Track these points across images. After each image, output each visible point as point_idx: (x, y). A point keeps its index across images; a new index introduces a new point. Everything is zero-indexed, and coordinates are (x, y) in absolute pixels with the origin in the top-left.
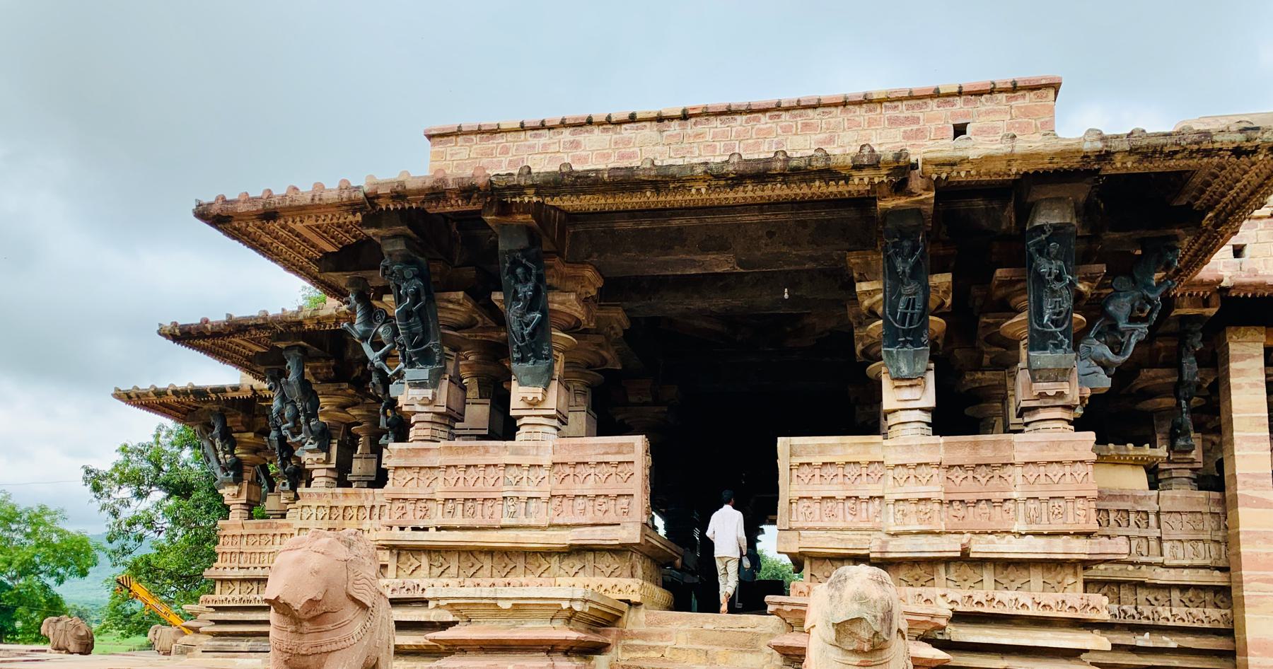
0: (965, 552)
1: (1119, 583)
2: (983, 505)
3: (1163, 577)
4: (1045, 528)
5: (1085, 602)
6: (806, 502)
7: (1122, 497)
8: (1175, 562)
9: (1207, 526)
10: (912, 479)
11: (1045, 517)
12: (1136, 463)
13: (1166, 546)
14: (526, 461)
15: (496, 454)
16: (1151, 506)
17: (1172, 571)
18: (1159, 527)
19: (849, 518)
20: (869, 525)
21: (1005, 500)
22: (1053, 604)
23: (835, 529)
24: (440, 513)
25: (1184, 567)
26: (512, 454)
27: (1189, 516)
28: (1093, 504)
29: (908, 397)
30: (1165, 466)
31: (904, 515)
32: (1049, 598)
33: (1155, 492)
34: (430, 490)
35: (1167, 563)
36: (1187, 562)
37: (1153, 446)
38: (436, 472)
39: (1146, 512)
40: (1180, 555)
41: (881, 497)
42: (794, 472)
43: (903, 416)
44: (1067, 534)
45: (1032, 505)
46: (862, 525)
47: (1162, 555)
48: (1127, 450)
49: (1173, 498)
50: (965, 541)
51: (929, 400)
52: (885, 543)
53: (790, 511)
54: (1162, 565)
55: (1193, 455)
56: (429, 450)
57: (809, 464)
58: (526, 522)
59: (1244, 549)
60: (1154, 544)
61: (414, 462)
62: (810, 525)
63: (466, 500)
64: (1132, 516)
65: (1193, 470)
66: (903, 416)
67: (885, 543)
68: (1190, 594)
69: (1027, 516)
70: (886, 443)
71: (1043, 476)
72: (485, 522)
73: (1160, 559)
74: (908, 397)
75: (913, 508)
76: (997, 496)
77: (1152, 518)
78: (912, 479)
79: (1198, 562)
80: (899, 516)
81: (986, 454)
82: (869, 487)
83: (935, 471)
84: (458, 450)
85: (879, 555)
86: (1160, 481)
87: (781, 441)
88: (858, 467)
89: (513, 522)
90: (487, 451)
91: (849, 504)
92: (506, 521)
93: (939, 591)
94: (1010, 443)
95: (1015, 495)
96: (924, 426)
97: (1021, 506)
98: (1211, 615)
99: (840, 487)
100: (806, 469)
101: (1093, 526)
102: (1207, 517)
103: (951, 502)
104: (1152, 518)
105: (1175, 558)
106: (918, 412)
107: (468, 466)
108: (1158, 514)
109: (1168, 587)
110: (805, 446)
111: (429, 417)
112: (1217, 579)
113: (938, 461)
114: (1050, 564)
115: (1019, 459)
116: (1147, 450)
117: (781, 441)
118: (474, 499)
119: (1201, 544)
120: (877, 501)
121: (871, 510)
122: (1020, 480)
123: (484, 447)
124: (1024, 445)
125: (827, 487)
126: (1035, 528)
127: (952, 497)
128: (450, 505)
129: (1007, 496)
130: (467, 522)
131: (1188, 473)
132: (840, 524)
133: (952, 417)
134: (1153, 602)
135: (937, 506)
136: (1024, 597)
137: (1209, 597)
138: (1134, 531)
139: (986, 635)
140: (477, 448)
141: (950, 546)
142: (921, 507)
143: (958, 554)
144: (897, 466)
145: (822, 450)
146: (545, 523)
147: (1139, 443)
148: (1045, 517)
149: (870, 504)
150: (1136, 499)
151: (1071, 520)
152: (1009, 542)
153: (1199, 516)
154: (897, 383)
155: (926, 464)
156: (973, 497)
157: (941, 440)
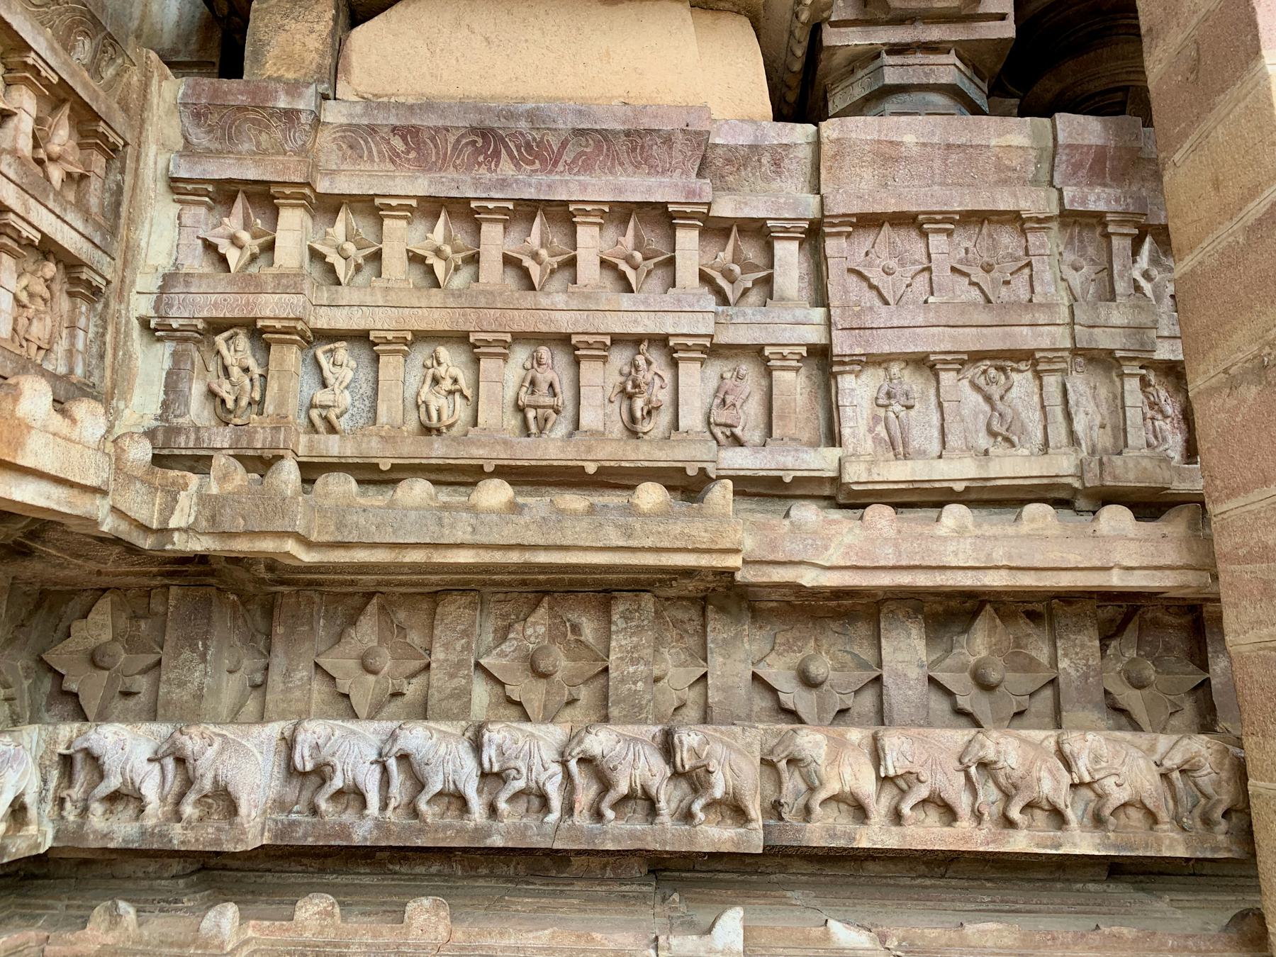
1: (603, 590)
3: (830, 552)
7: (636, 141)
8: (898, 472)
9: (1047, 287)
13: (857, 391)
16: (784, 199)
17: (880, 515)
18: (821, 299)
27: (965, 240)
35: (855, 474)
36: (957, 470)
40: (924, 433)
47: (833, 438)
49: (887, 155)
60: (794, 385)
64: (687, 239)
68: (979, 644)
73: (821, 461)
102: (1048, 243)
104: (788, 254)
105: (897, 446)
109: (855, 610)
112: (1125, 553)
119: (1022, 381)
134: (792, 695)
137: (1074, 655)
138: (691, 315)
153: (1007, 239)
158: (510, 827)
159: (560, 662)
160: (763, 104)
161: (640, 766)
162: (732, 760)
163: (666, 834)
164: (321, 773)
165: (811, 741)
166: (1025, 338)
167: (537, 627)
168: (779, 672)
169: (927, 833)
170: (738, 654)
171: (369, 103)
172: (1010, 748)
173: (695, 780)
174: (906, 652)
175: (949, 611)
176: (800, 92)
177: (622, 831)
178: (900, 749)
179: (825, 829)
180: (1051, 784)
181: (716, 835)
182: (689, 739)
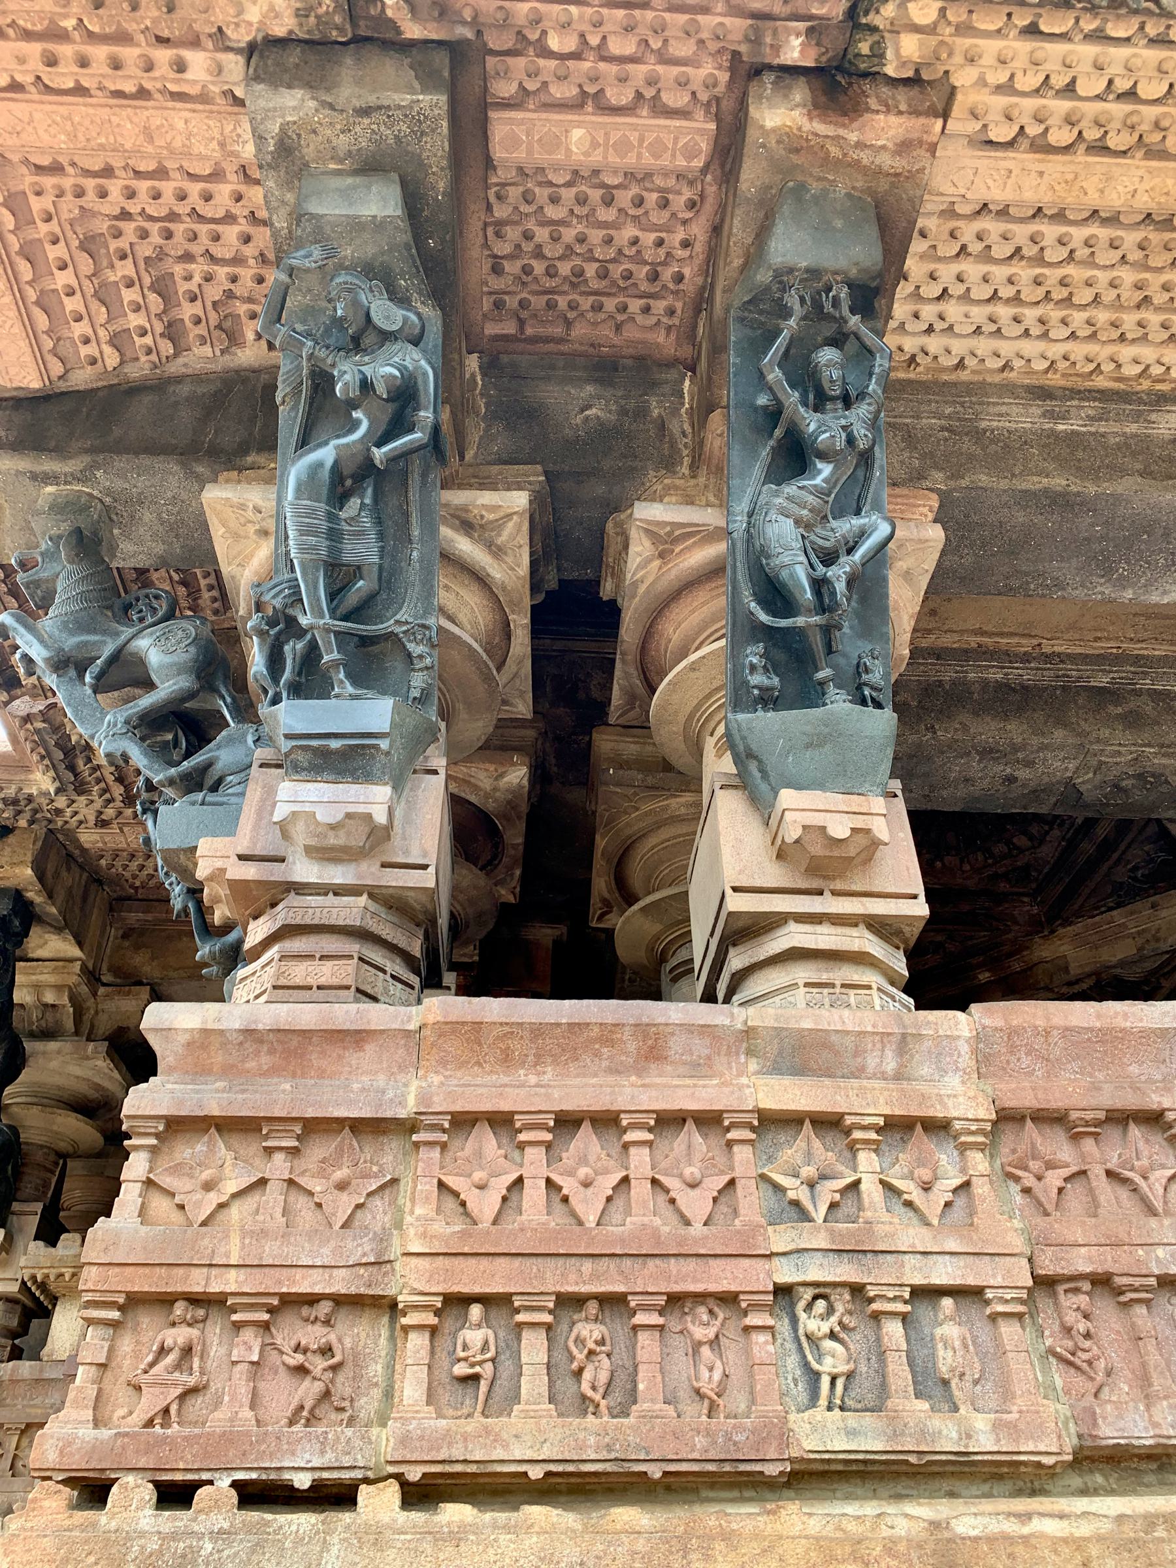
14: (868, 1101)
15: (699, 1068)
24: (412, 1390)
26: (776, 1069)
34: (361, 1249)
38: (388, 1156)
56: (357, 1037)
58: (946, 1435)
61: (280, 1096)
63: (570, 1302)
72: (697, 1443)
84: (506, 1049)
89: (865, 1437)
90: (653, 1049)
92: (823, 1433)
107: (567, 1122)
111: (351, 911)
118: (613, 1302)
123: (642, 1029)
128: (475, 1334)
130: (587, 1442)
140: (608, 1034)
146: (1050, 1443)
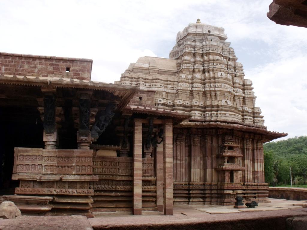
0: (61, 179)
2: (66, 167)
4: (80, 173)
5: (88, 191)
6: (22, 166)
8: (122, 175)
10: (49, 160)
11: (80, 171)
12: (114, 150)
13: (120, 170)
18: (119, 166)
19: (33, 170)
20: (37, 172)
21: (72, 166)
22: (81, 192)
23: (29, 173)
25: (124, 176)
27: (126, 163)
28: (92, 167)
29: (50, 139)
30: (121, 151)
31: (47, 169)
32: (80, 191)
33: (118, 157)
35: (120, 175)
36: (124, 174)
37: (119, 146)
39: (116, 162)
40: (123, 172)
41: (41, 165)
42: (19, 157)
43: (48, 143)
44: (85, 175)
45: (78, 167)
46: (36, 172)
48: (112, 147)
50: (61, 176)
51: (55, 140)
52: (41, 177)
53: (17, 167)
54: (119, 175)
55: (127, 148)
57: (23, 155)
59: (135, 172)
60: (117, 170)
62: (22, 172)
64: (113, 163)
65: (127, 152)
66: (48, 143)
67: (41, 177)
69: (76, 170)
70: (44, 150)
71: (81, 161)
73: (119, 174)
74: (50, 139)
75: (49, 167)
76: (69, 165)
77: (117, 163)
78: (49, 160)
79: (127, 174)
80: (46, 169)
81: (68, 154)
82: (38, 162)
83: (55, 158)
85: (39, 180)
86: (120, 154)
87: (15, 148)
88: (36, 156)
91: (32, 166)
93: (54, 189)
94: (74, 152)
95: (74, 165)
96: (54, 146)
97: (75, 168)
98: (127, 187)
99: (31, 162)
100: (22, 156)
101: (92, 173)
103: (59, 166)
104: (117, 163)
106: (52, 142)
108: (119, 162)
109: (120, 181)
110: (22, 150)
112: (130, 179)
113: (56, 155)
114: (82, 183)
115: (75, 155)
116: (117, 147)
117: (15, 148)
120: (40, 166)
121: (38, 168)
122: (75, 161)
124: (77, 152)
125: (27, 162)
126: (78, 173)
127: (59, 165)
129: (72, 165)
131: (126, 152)
132: (30, 172)
133: (61, 144)
135: (55, 167)
136: (74, 191)
137: (128, 183)
139: (65, 200)
141: (57, 178)
142: (51, 167)
143: (59, 180)
144: (46, 156)
145: (27, 151)
147: (115, 145)
148: (80, 171)
149: (38, 167)
150: (114, 159)
151: (86, 171)
152: (71, 177)
154: (47, 135)
155: (53, 156)
156: (63, 165)
157: (57, 150)
158: (106, 189)
159: (106, 183)
160: (116, 156)
161: (111, 187)
162: (114, 187)
163: (112, 190)
164: (98, 187)
165: (117, 186)
166: (128, 168)
167: (105, 181)
168: (116, 183)
169: (121, 190)
170: (114, 183)
171: (98, 156)
172: (125, 186)
173: (113, 188)
174: (121, 183)
175: (123, 181)
176: (118, 155)
177: (110, 189)
178: (121, 186)
179: (118, 189)
180: (126, 188)
181: (113, 190)
182: (113, 186)
